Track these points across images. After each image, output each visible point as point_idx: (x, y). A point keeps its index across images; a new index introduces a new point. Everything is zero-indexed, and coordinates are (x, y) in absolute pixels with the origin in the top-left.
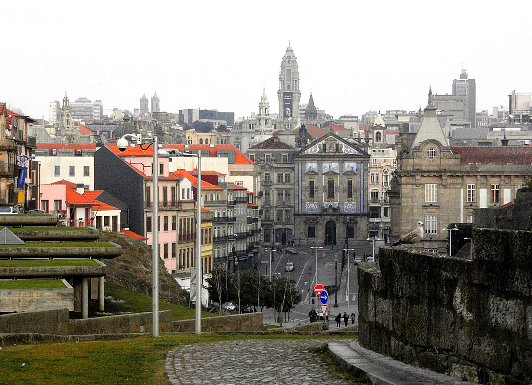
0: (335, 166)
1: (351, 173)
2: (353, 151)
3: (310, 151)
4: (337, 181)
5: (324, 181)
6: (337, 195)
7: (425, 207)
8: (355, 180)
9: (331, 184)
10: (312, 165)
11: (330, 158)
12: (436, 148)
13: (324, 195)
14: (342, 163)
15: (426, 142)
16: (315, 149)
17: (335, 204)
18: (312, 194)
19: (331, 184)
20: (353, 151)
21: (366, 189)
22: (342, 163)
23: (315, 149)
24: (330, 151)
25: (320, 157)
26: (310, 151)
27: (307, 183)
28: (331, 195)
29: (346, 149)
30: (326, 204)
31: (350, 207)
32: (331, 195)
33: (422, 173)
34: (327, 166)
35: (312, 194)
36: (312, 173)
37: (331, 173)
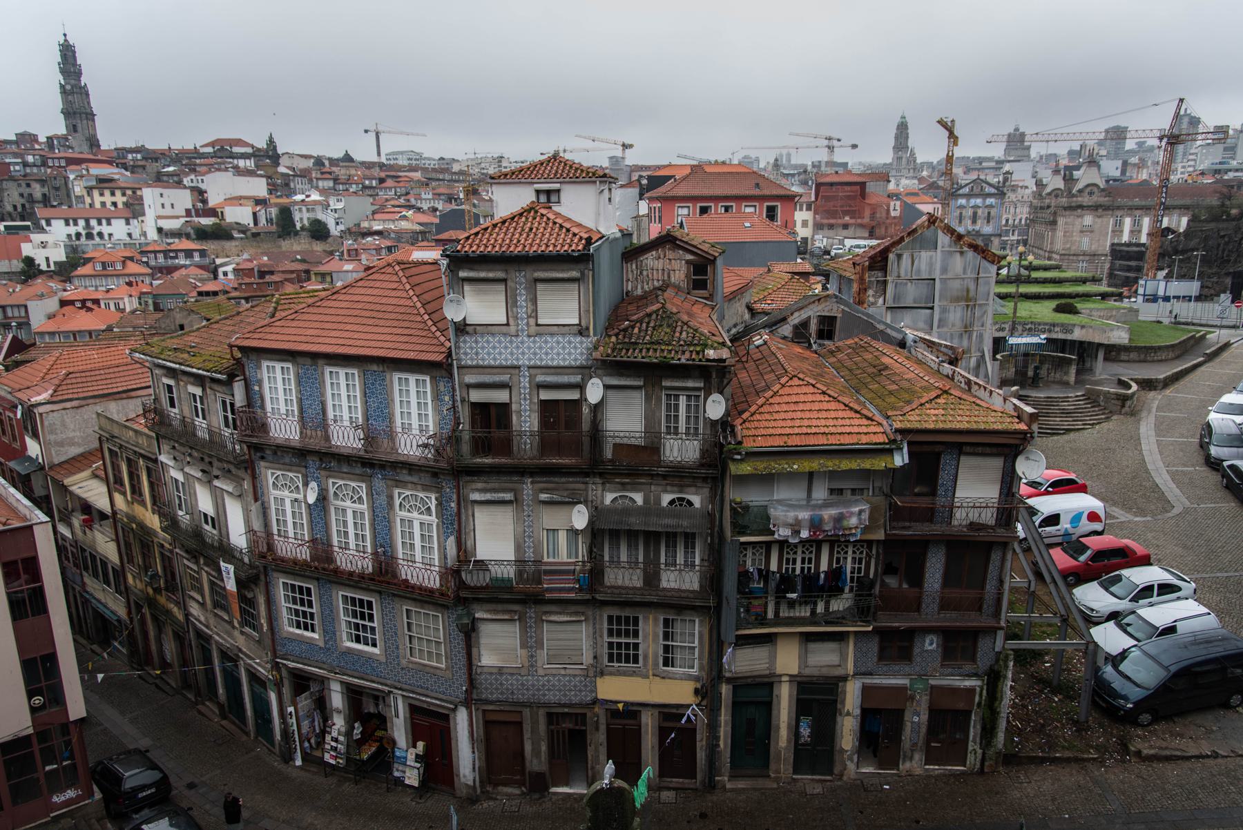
0: (979, 201)
1: (991, 206)
2: (993, 191)
3: (961, 192)
4: (980, 212)
5: (970, 212)
6: (979, 222)
7: (1082, 232)
8: (993, 212)
9: (975, 214)
10: (962, 201)
11: (977, 196)
12: (1095, 190)
13: (969, 222)
14: (984, 200)
15: (1088, 185)
16: (966, 190)
17: (977, 228)
18: (960, 222)
19: (975, 214)
20: (993, 191)
21: (1000, 217)
22: (984, 200)
23: (966, 190)
24: (976, 191)
25: (968, 196)
26: (961, 192)
27: (957, 213)
28: (974, 222)
29: (988, 190)
30: (970, 228)
31: (987, 229)
32: (974, 222)
33: (1081, 207)
34: (973, 202)
35: (960, 222)
36: (962, 207)
37: (976, 207)
